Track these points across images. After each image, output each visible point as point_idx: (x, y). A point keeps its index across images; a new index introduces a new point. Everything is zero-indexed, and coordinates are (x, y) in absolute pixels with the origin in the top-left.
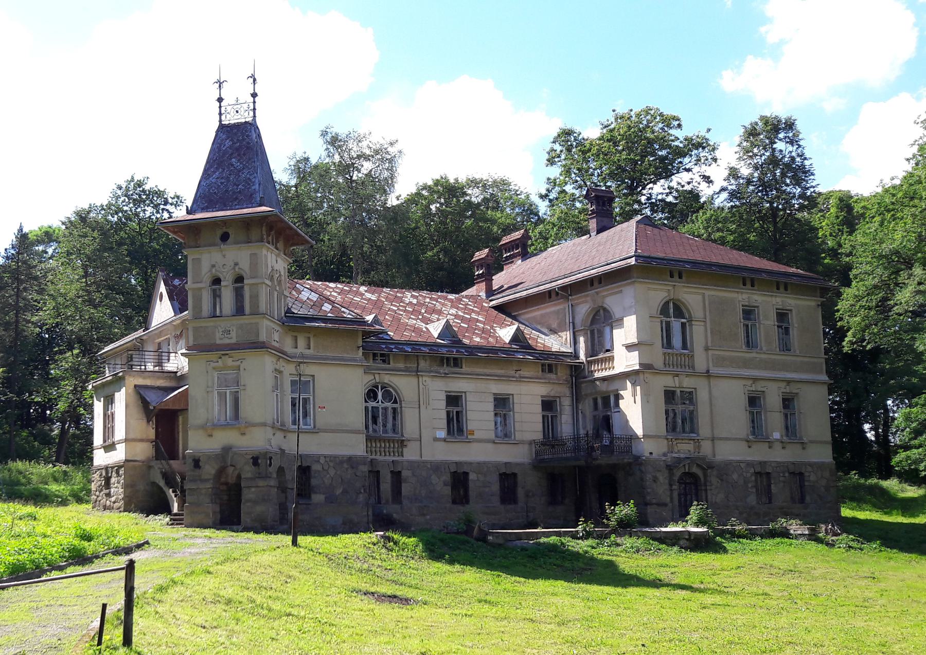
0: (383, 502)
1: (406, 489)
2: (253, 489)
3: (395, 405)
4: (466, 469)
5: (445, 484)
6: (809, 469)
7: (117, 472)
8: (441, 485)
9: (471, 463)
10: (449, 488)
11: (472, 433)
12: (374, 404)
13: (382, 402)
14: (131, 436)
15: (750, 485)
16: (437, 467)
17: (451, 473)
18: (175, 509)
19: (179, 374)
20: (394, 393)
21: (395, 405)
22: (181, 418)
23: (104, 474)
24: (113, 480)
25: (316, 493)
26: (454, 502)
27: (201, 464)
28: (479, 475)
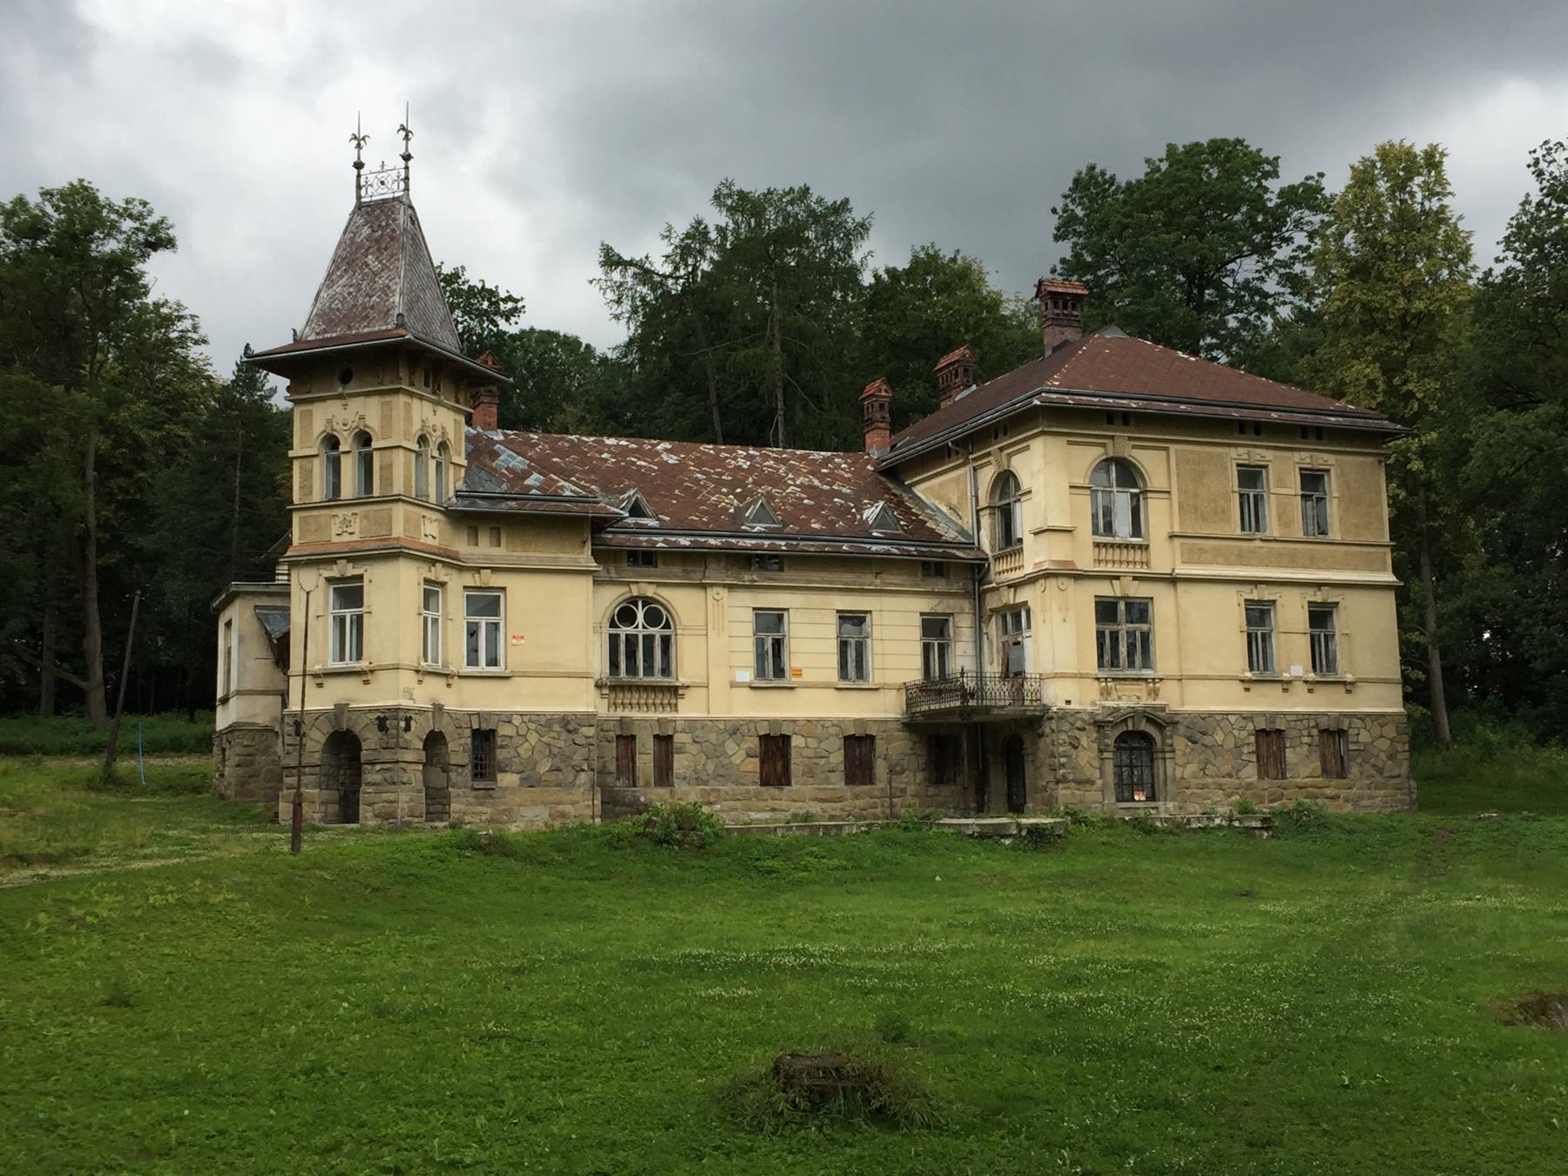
0: (641, 782)
1: (680, 763)
2: (378, 767)
3: (666, 632)
6: (1358, 723)
8: (743, 758)
9: (794, 721)
10: (757, 760)
11: (798, 673)
12: (630, 630)
14: (248, 686)
15: (1245, 750)
16: (735, 729)
17: (760, 737)
20: (664, 612)
21: (666, 632)
26: (765, 782)
28: (810, 740)
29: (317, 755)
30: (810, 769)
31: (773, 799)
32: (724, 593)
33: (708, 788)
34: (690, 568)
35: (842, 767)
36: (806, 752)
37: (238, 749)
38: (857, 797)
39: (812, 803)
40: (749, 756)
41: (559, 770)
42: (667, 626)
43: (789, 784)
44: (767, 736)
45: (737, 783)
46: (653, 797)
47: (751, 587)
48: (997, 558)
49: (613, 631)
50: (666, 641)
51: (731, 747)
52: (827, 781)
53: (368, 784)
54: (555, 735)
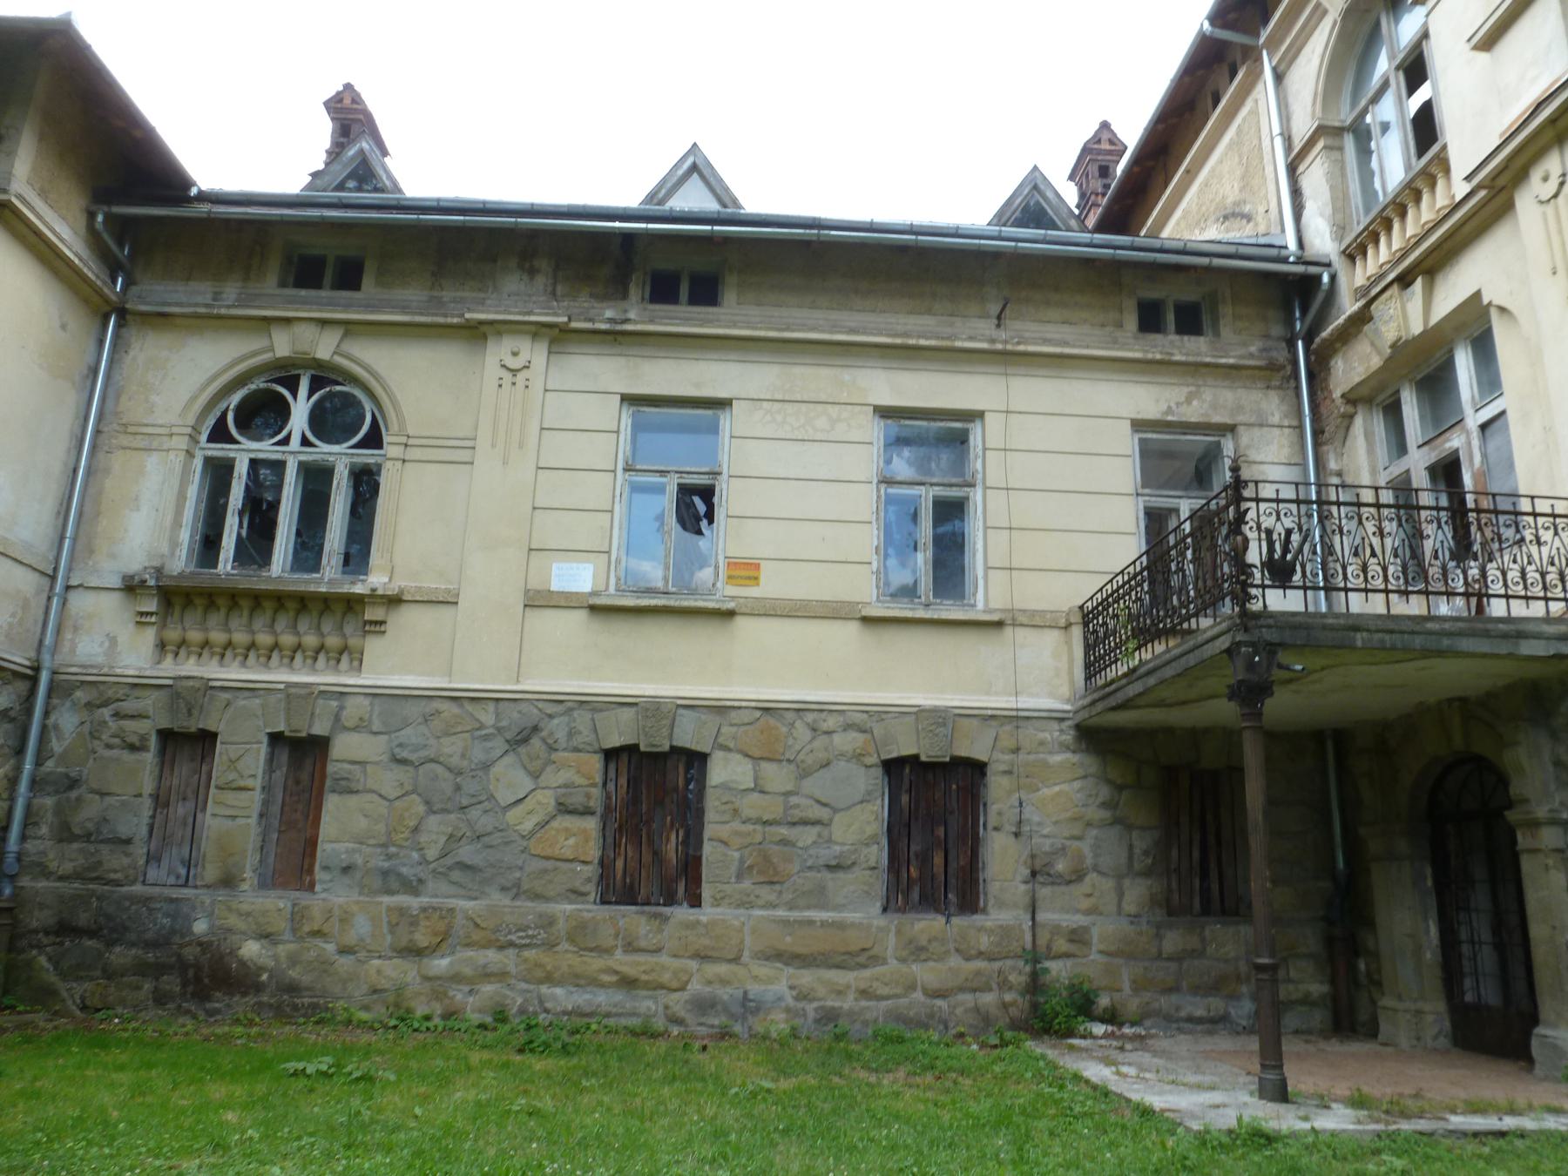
3: (367, 456)
4: (688, 735)
9: (720, 709)
10: (591, 824)
12: (265, 448)
13: (305, 442)
20: (368, 407)
21: (367, 456)
28: (769, 769)
30: (766, 858)
31: (631, 947)
32: (534, 354)
33: (413, 902)
34: (447, 295)
35: (878, 854)
36: (752, 805)
38: (917, 951)
39: (763, 970)
40: (564, 809)
42: (374, 440)
43: (696, 902)
44: (632, 749)
45: (516, 890)
46: (233, 921)
47: (615, 339)
48: (1354, 253)
49: (219, 450)
50: (366, 484)
51: (509, 779)
52: (819, 898)
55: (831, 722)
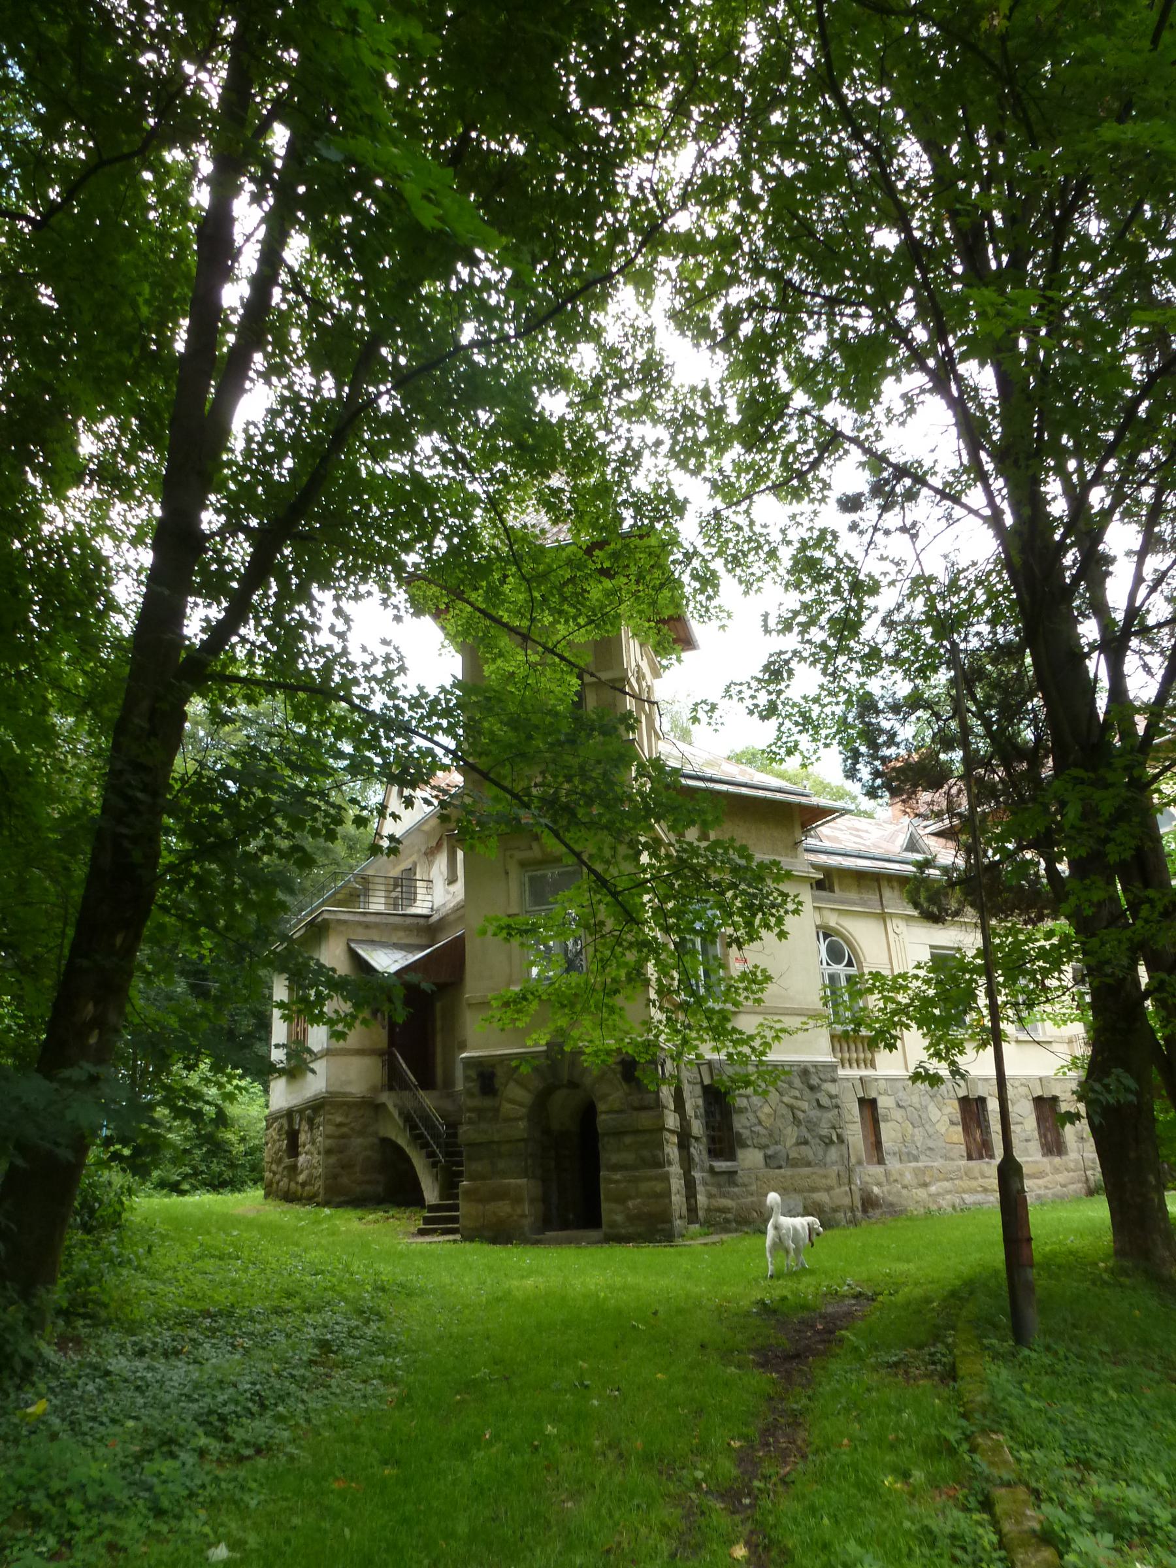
1: (887, 1132)
2: (628, 1140)
3: (853, 971)
5: (952, 1123)
7: (311, 1122)
10: (960, 1128)
18: (431, 1194)
19: (435, 918)
22: (438, 1005)
23: (286, 1127)
24: (303, 1138)
25: (744, 1146)
26: (970, 1158)
27: (498, 1082)
29: (522, 1125)
33: (920, 1164)
35: (1036, 1134)
37: (330, 1129)
38: (1057, 1171)
41: (806, 1143)
46: (867, 1179)
53: (615, 1168)
54: (797, 1094)
55: (1017, 1084)
